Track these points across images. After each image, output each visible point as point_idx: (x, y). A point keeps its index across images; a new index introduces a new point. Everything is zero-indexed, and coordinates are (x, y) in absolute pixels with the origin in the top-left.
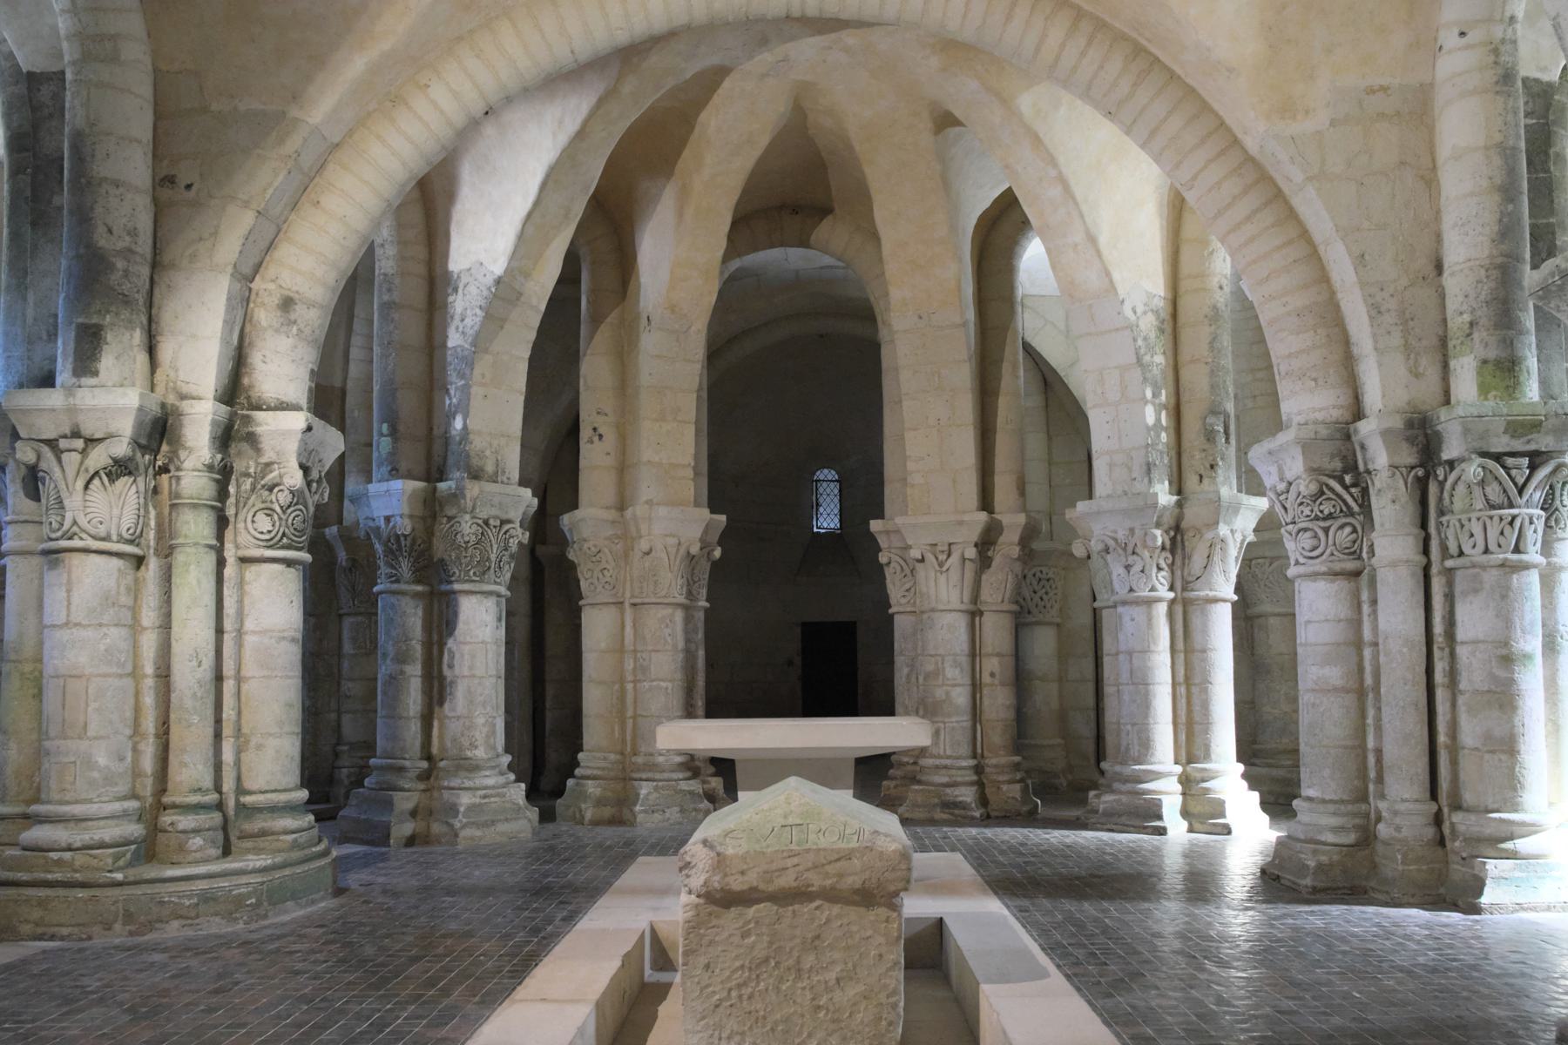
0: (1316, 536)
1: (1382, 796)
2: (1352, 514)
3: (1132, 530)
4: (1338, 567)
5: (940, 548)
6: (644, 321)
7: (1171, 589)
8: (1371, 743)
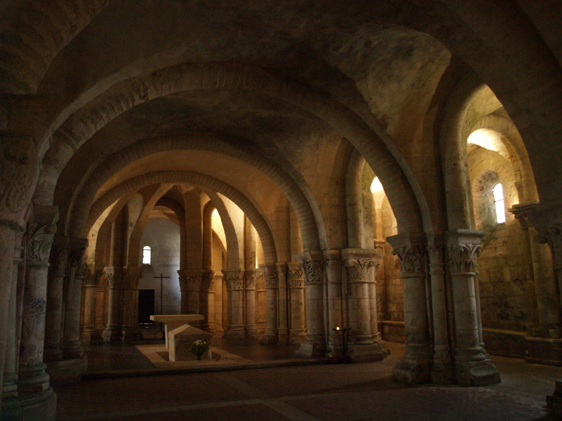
0: (269, 282)
1: (279, 327)
2: (275, 278)
3: (235, 276)
4: (273, 287)
5: (194, 277)
6: (129, 224)
7: (243, 288)
8: (278, 318)
